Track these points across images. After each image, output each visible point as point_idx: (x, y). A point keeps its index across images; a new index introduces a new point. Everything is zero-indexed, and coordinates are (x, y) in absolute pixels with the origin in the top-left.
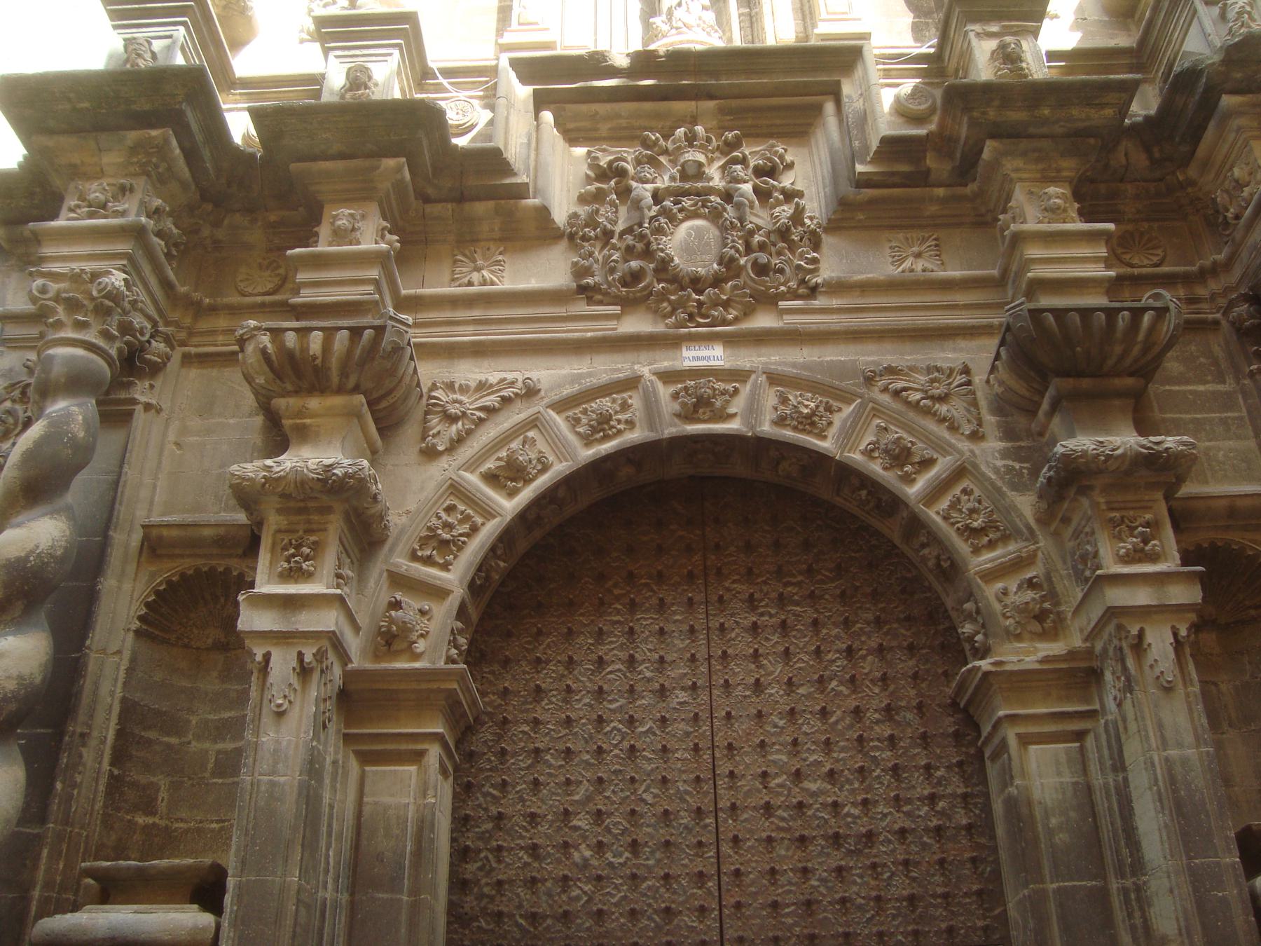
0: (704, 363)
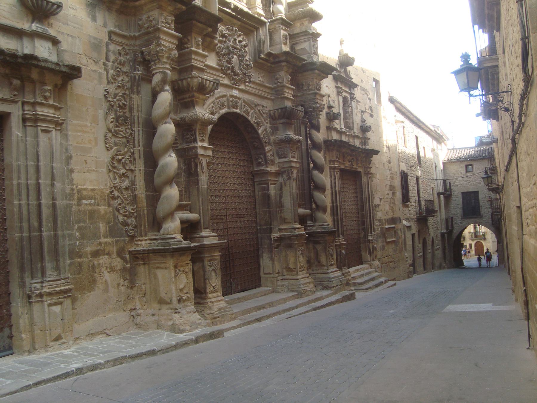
0: (235, 94)
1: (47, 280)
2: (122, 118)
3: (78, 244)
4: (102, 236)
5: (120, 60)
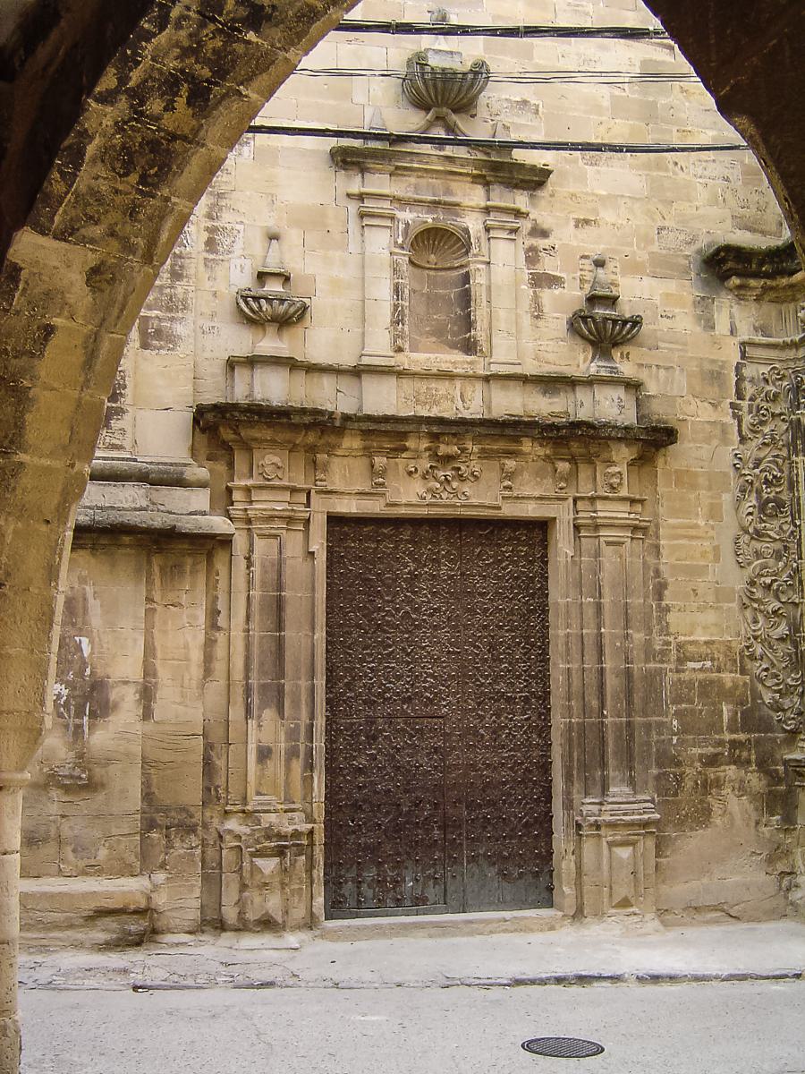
1: (610, 800)
2: (770, 505)
3: (675, 741)
4: (725, 728)
5: (766, 393)
